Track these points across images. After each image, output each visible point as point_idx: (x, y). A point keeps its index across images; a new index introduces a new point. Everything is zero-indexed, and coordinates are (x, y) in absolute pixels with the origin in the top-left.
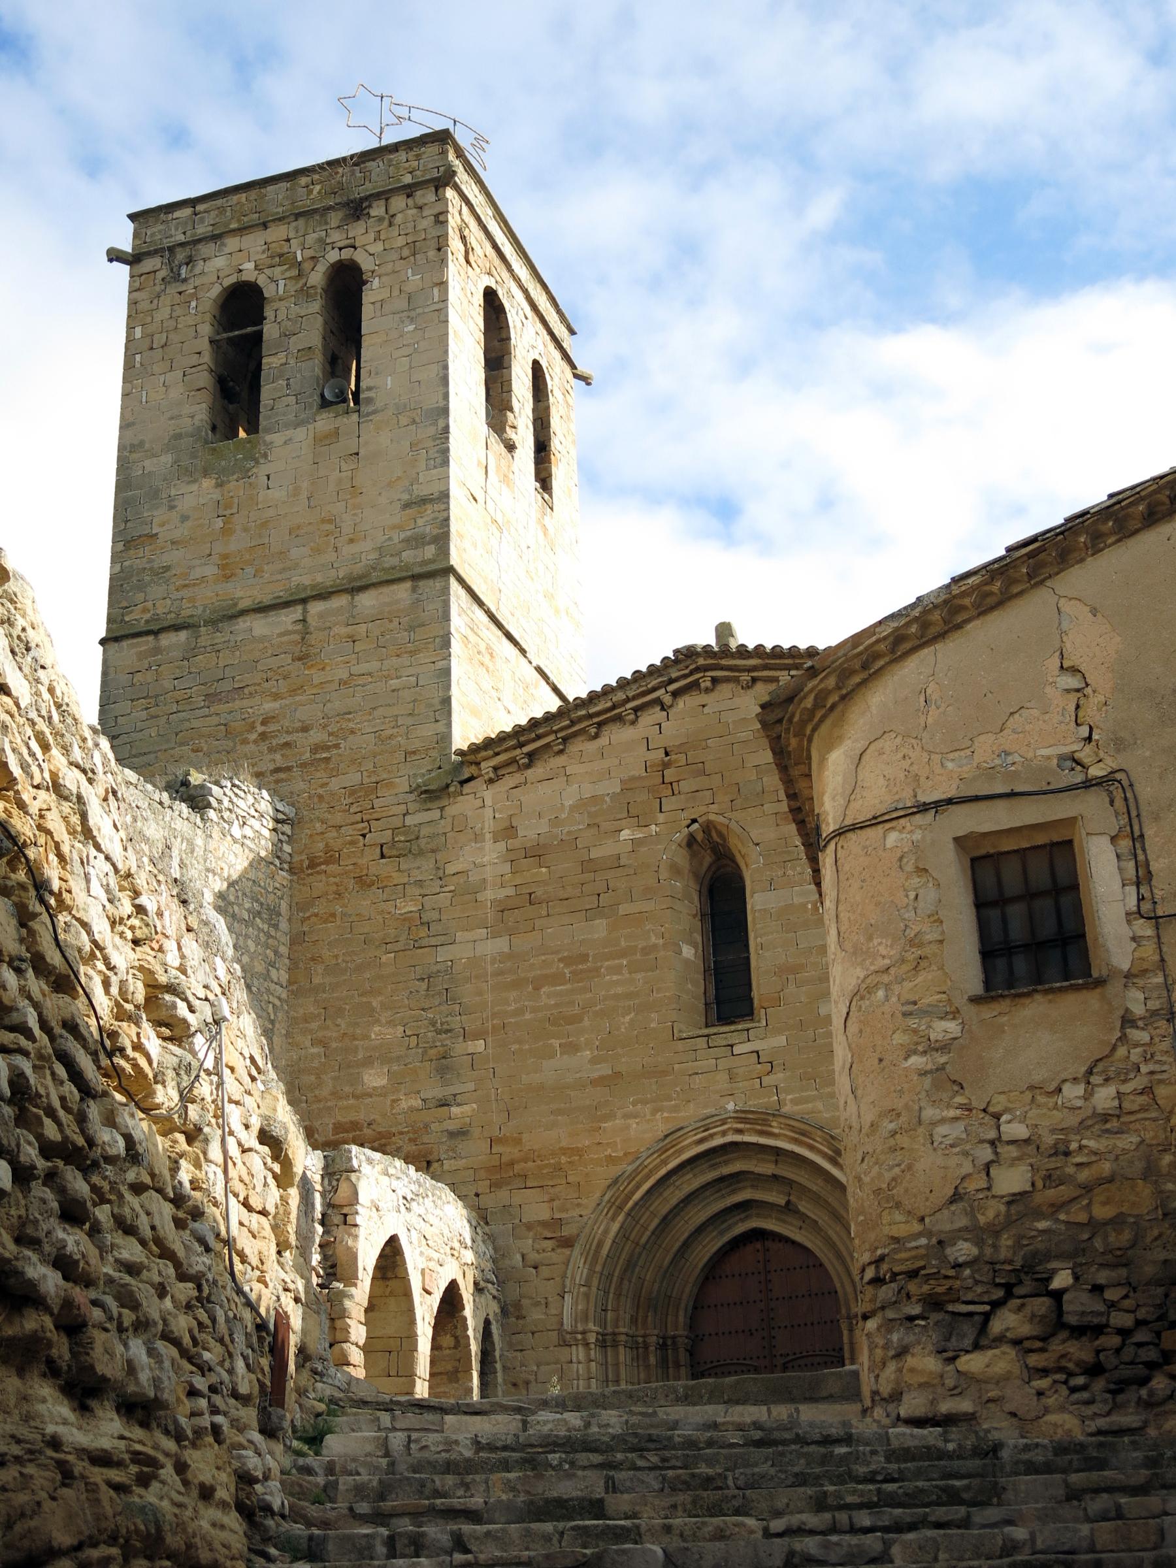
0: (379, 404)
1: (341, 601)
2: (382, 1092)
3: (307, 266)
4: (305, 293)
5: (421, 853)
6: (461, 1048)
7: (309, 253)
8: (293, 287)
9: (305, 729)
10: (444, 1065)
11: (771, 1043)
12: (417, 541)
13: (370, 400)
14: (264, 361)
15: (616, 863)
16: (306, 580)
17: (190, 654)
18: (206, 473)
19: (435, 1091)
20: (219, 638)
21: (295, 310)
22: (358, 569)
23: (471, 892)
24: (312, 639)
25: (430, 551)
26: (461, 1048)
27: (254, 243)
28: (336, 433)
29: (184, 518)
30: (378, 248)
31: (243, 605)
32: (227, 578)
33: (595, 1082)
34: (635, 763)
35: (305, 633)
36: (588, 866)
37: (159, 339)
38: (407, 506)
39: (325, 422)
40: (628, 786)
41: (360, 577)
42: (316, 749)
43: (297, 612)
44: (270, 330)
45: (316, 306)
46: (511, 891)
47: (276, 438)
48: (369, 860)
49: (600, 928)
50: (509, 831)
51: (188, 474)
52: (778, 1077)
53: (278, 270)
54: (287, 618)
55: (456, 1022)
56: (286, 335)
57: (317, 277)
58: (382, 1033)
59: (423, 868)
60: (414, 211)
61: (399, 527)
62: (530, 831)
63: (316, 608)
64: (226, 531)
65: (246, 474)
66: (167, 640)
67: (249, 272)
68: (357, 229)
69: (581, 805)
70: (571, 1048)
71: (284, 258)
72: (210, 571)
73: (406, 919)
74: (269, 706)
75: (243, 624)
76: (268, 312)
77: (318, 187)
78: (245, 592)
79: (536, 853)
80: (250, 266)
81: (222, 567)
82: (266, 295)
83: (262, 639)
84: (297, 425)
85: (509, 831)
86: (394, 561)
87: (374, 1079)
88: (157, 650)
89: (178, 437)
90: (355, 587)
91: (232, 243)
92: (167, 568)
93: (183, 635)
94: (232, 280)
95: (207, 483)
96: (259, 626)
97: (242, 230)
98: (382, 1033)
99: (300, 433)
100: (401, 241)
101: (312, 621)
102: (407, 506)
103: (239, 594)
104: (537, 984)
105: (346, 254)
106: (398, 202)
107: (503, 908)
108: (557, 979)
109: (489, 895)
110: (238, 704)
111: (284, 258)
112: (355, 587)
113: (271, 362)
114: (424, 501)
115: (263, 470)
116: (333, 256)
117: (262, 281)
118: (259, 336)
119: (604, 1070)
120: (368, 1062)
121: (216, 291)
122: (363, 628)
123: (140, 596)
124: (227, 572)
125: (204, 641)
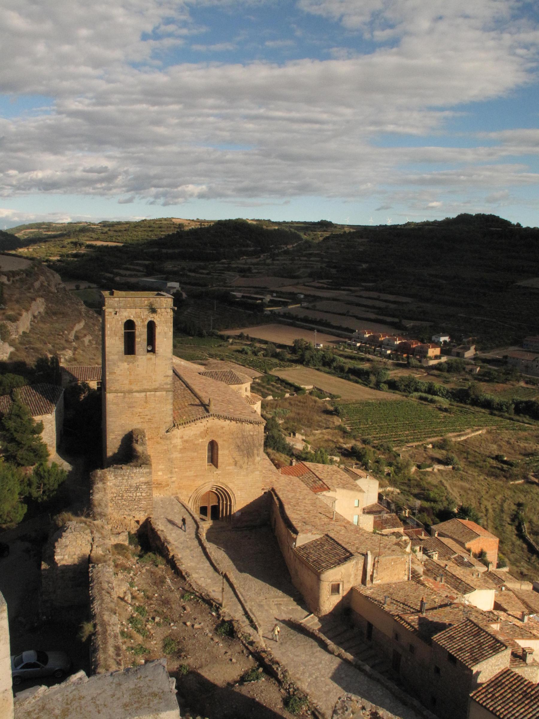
0: (159, 354)
1: (153, 393)
2: (161, 475)
3: (144, 320)
4: (143, 326)
5: (167, 439)
6: (174, 470)
7: (145, 317)
8: (142, 324)
9: (147, 415)
10: (171, 472)
11: (219, 472)
12: (166, 384)
13: (157, 353)
14: (136, 339)
15: (198, 444)
16: (146, 387)
17: (124, 397)
18: (125, 361)
19: (169, 476)
20: (130, 396)
21: (142, 329)
22: (156, 387)
23: (175, 447)
24: (148, 399)
25: (169, 386)
26: (174, 470)
27: (133, 311)
28: (150, 359)
29: (121, 370)
30: (159, 320)
31: (134, 390)
32: (131, 384)
33: (195, 476)
34: (202, 429)
35: (146, 398)
36: (194, 444)
37: (114, 329)
38: (165, 376)
39: (150, 355)
40: (201, 432)
41: (156, 389)
42: (149, 419)
43: (144, 393)
44: (137, 333)
45: (146, 330)
46: (182, 447)
47: (139, 357)
48: (159, 439)
49: (196, 454)
50: (182, 438)
51: (122, 361)
52: (219, 477)
53: (138, 319)
54: (143, 394)
55: (173, 466)
56: (140, 335)
57: (146, 323)
58: (160, 467)
59: (168, 442)
60: (166, 313)
61: (163, 381)
62: (186, 438)
63: (148, 393)
64: (130, 375)
65: (133, 363)
66: (119, 394)
67: (132, 318)
68: (154, 315)
69: (194, 435)
70: (190, 471)
71: (139, 317)
72: (127, 382)
73: (165, 449)
74: (140, 410)
75: (135, 394)
76: (137, 328)
77: (146, 302)
78: (135, 388)
79: (186, 441)
80: (132, 317)
81: (130, 382)
82: (136, 324)
83: (138, 398)
84: (143, 355)
85: (182, 438)
86: (162, 387)
87: (160, 473)
88: (117, 396)
89: (118, 352)
90: (155, 390)
91: (128, 310)
92: (118, 380)
93: (122, 394)
94: (128, 319)
95: (126, 364)
96: (137, 395)
97: (130, 308)
98: (160, 467)
99: (144, 357)
100: (163, 319)
101: (148, 396)
102: (165, 376)
103: (133, 387)
104: (186, 461)
105: (152, 319)
106: (163, 310)
107: (181, 449)
108: (189, 461)
109: (179, 447)
110: (134, 409)
111: (139, 317)
112: (155, 390)
113: (137, 340)
114: (168, 376)
115: (136, 363)
116: (150, 319)
117: (135, 321)
118: (134, 334)
119: (195, 474)
120: (159, 471)
121: (125, 320)
122: (157, 399)
123: (113, 385)
124: (131, 383)
125: (127, 396)
